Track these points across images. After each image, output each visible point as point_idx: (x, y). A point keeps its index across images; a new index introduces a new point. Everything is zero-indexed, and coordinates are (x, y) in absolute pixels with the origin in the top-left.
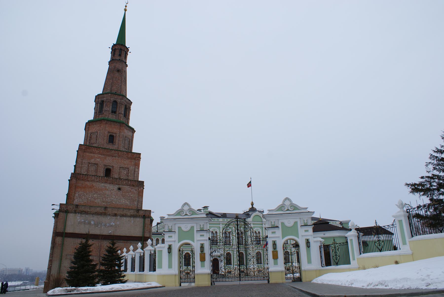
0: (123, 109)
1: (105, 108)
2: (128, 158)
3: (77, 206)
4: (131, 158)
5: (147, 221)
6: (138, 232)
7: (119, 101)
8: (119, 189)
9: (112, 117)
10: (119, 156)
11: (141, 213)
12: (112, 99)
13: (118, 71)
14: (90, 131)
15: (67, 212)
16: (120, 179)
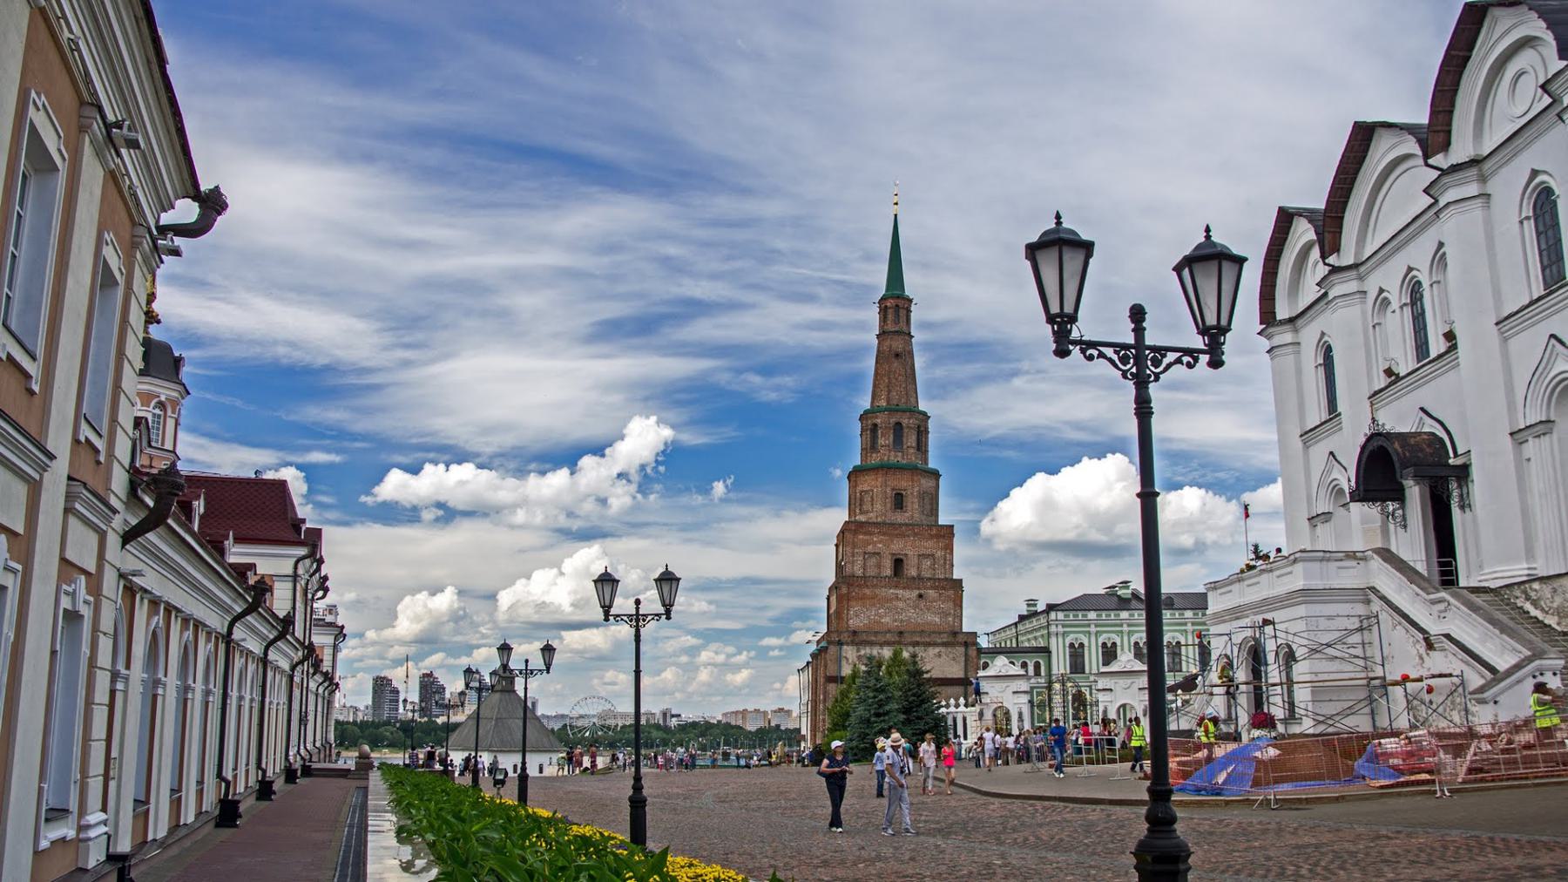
0: (914, 437)
1: (881, 441)
2: (932, 537)
3: (855, 632)
4: (938, 536)
5: (972, 652)
6: (956, 671)
7: (905, 422)
8: (920, 596)
9: (896, 458)
10: (915, 534)
11: (960, 638)
12: (893, 420)
13: (897, 355)
14: (859, 488)
15: (840, 643)
16: (920, 578)
